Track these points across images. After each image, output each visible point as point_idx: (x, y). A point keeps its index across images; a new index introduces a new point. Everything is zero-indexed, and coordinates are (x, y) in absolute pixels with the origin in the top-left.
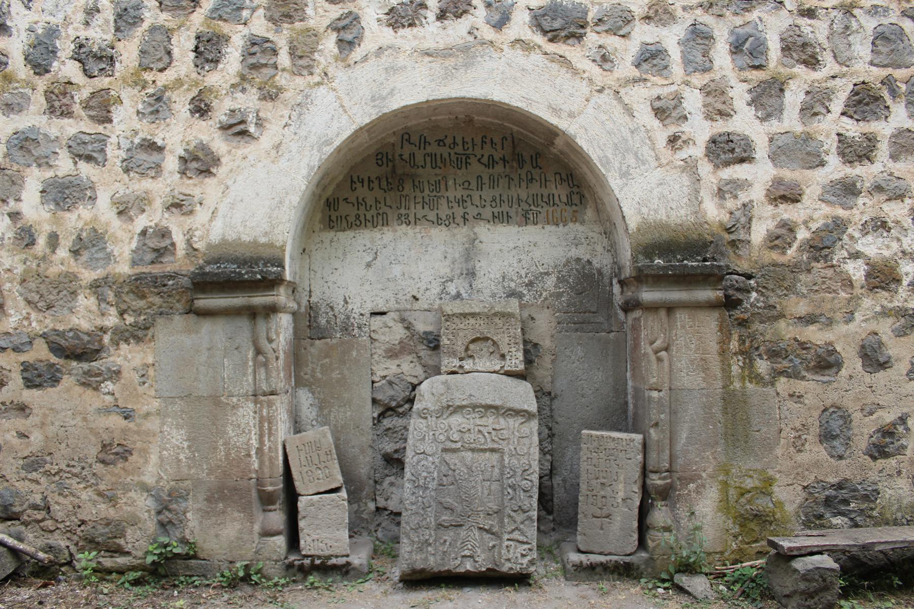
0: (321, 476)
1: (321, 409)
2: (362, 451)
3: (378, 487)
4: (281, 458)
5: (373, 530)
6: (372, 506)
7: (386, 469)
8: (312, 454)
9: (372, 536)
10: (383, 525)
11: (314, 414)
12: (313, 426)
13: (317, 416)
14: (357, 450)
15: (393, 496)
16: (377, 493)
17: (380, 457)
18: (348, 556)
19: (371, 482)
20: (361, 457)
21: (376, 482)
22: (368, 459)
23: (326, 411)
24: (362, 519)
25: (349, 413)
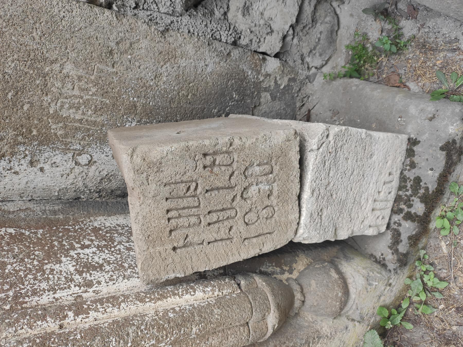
0: (265, 187)
1: (46, 140)
2: (169, 56)
3: (244, 41)
4: (200, 295)
5: (306, 73)
6: (272, 65)
7: (212, 13)
8: (203, 210)
9: (315, 75)
10: (305, 51)
11: (58, 158)
12: (90, 163)
13: (65, 151)
14: (166, 70)
15: (267, 15)
16: (254, 47)
17: (186, 19)
18: (413, 142)
19: (236, 53)
20: (183, 63)
21: (235, 44)
22: (190, 49)
23: (56, 129)
24: (288, 87)
25: (69, 68)
